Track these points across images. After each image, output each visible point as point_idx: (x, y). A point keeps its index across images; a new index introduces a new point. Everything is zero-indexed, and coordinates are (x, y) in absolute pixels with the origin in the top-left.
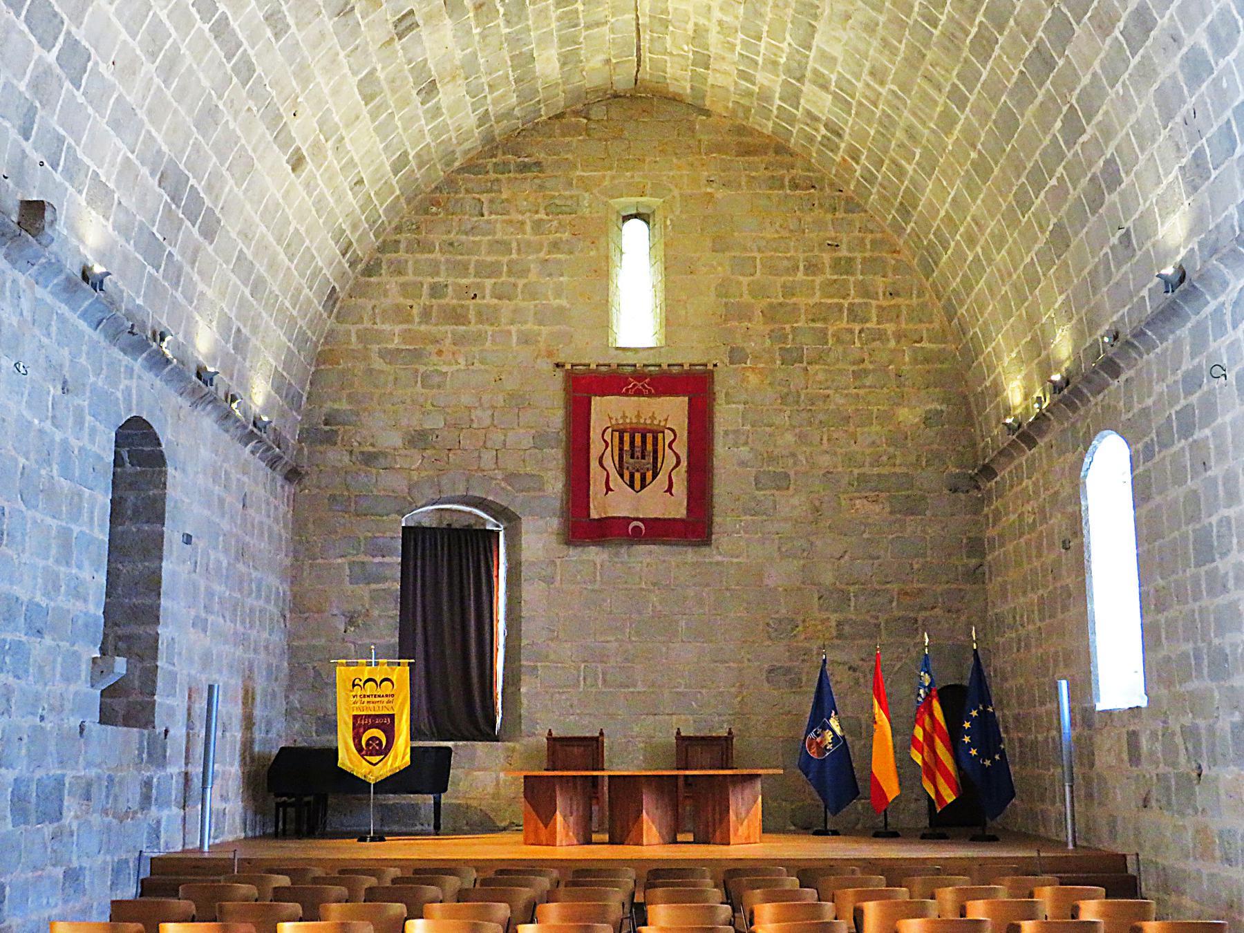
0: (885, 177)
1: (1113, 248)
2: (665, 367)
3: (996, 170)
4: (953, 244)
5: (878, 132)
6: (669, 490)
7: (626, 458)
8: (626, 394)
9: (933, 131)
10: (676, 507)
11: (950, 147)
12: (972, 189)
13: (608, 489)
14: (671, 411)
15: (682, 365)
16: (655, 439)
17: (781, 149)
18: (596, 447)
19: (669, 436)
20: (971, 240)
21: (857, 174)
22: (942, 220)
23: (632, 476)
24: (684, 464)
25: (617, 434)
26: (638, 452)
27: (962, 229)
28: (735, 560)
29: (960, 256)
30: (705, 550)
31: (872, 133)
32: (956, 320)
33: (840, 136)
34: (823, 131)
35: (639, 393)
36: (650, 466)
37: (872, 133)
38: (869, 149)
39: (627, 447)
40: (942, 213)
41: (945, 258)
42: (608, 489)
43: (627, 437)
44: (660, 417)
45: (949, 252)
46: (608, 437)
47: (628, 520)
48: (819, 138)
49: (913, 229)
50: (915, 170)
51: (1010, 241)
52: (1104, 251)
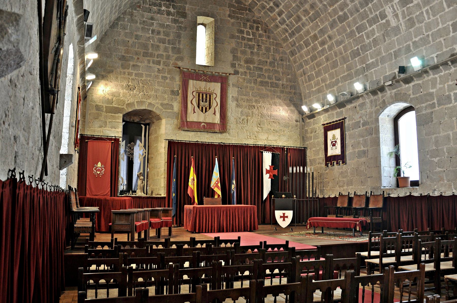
0: (291, 22)
1: (414, 43)
2: (214, 73)
3: (350, 19)
4: (312, 45)
5: (297, 6)
6: (215, 114)
7: (201, 102)
8: (201, 80)
9: (324, 5)
10: (217, 119)
11: (329, 11)
12: (332, 25)
13: (194, 112)
14: (216, 88)
15: (219, 73)
16: (210, 96)
17: (250, 10)
18: (190, 97)
19: (215, 96)
20: (323, 43)
21: (277, 21)
22: (310, 37)
23: (202, 108)
24: (219, 105)
25: (197, 94)
26: (204, 99)
27: (320, 40)
28: (234, 138)
29: (314, 48)
30: (224, 134)
31: (294, 5)
32: (302, 70)
33: (278, 6)
34: (272, 4)
35: (205, 81)
36: (208, 105)
37: (294, 5)
38: (289, 12)
39: (201, 98)
40: (312, 34)
41: (305, 49)
42: (194, 112)
43: (201, 95)
44: (212, 89)
45: (308, 48)
46: (194, 93)
47: (200, 123)
48: (268, 7)
49: (293, 40)
50: (307, 19)
51: (347, 42)
52: (408, 43)
